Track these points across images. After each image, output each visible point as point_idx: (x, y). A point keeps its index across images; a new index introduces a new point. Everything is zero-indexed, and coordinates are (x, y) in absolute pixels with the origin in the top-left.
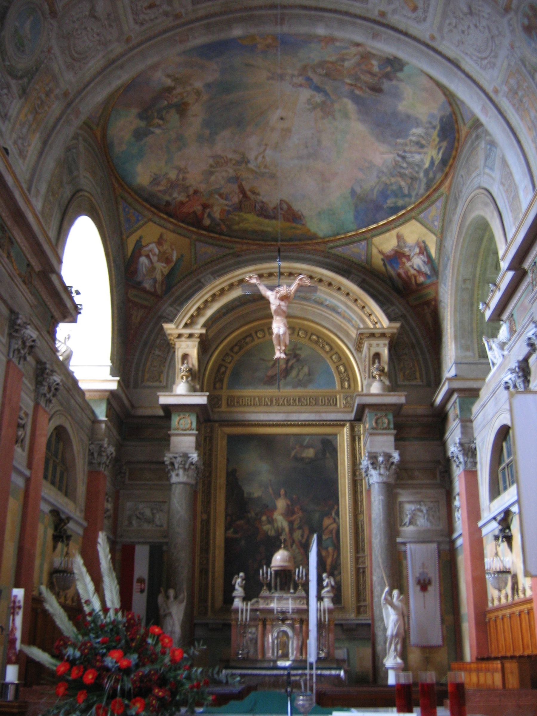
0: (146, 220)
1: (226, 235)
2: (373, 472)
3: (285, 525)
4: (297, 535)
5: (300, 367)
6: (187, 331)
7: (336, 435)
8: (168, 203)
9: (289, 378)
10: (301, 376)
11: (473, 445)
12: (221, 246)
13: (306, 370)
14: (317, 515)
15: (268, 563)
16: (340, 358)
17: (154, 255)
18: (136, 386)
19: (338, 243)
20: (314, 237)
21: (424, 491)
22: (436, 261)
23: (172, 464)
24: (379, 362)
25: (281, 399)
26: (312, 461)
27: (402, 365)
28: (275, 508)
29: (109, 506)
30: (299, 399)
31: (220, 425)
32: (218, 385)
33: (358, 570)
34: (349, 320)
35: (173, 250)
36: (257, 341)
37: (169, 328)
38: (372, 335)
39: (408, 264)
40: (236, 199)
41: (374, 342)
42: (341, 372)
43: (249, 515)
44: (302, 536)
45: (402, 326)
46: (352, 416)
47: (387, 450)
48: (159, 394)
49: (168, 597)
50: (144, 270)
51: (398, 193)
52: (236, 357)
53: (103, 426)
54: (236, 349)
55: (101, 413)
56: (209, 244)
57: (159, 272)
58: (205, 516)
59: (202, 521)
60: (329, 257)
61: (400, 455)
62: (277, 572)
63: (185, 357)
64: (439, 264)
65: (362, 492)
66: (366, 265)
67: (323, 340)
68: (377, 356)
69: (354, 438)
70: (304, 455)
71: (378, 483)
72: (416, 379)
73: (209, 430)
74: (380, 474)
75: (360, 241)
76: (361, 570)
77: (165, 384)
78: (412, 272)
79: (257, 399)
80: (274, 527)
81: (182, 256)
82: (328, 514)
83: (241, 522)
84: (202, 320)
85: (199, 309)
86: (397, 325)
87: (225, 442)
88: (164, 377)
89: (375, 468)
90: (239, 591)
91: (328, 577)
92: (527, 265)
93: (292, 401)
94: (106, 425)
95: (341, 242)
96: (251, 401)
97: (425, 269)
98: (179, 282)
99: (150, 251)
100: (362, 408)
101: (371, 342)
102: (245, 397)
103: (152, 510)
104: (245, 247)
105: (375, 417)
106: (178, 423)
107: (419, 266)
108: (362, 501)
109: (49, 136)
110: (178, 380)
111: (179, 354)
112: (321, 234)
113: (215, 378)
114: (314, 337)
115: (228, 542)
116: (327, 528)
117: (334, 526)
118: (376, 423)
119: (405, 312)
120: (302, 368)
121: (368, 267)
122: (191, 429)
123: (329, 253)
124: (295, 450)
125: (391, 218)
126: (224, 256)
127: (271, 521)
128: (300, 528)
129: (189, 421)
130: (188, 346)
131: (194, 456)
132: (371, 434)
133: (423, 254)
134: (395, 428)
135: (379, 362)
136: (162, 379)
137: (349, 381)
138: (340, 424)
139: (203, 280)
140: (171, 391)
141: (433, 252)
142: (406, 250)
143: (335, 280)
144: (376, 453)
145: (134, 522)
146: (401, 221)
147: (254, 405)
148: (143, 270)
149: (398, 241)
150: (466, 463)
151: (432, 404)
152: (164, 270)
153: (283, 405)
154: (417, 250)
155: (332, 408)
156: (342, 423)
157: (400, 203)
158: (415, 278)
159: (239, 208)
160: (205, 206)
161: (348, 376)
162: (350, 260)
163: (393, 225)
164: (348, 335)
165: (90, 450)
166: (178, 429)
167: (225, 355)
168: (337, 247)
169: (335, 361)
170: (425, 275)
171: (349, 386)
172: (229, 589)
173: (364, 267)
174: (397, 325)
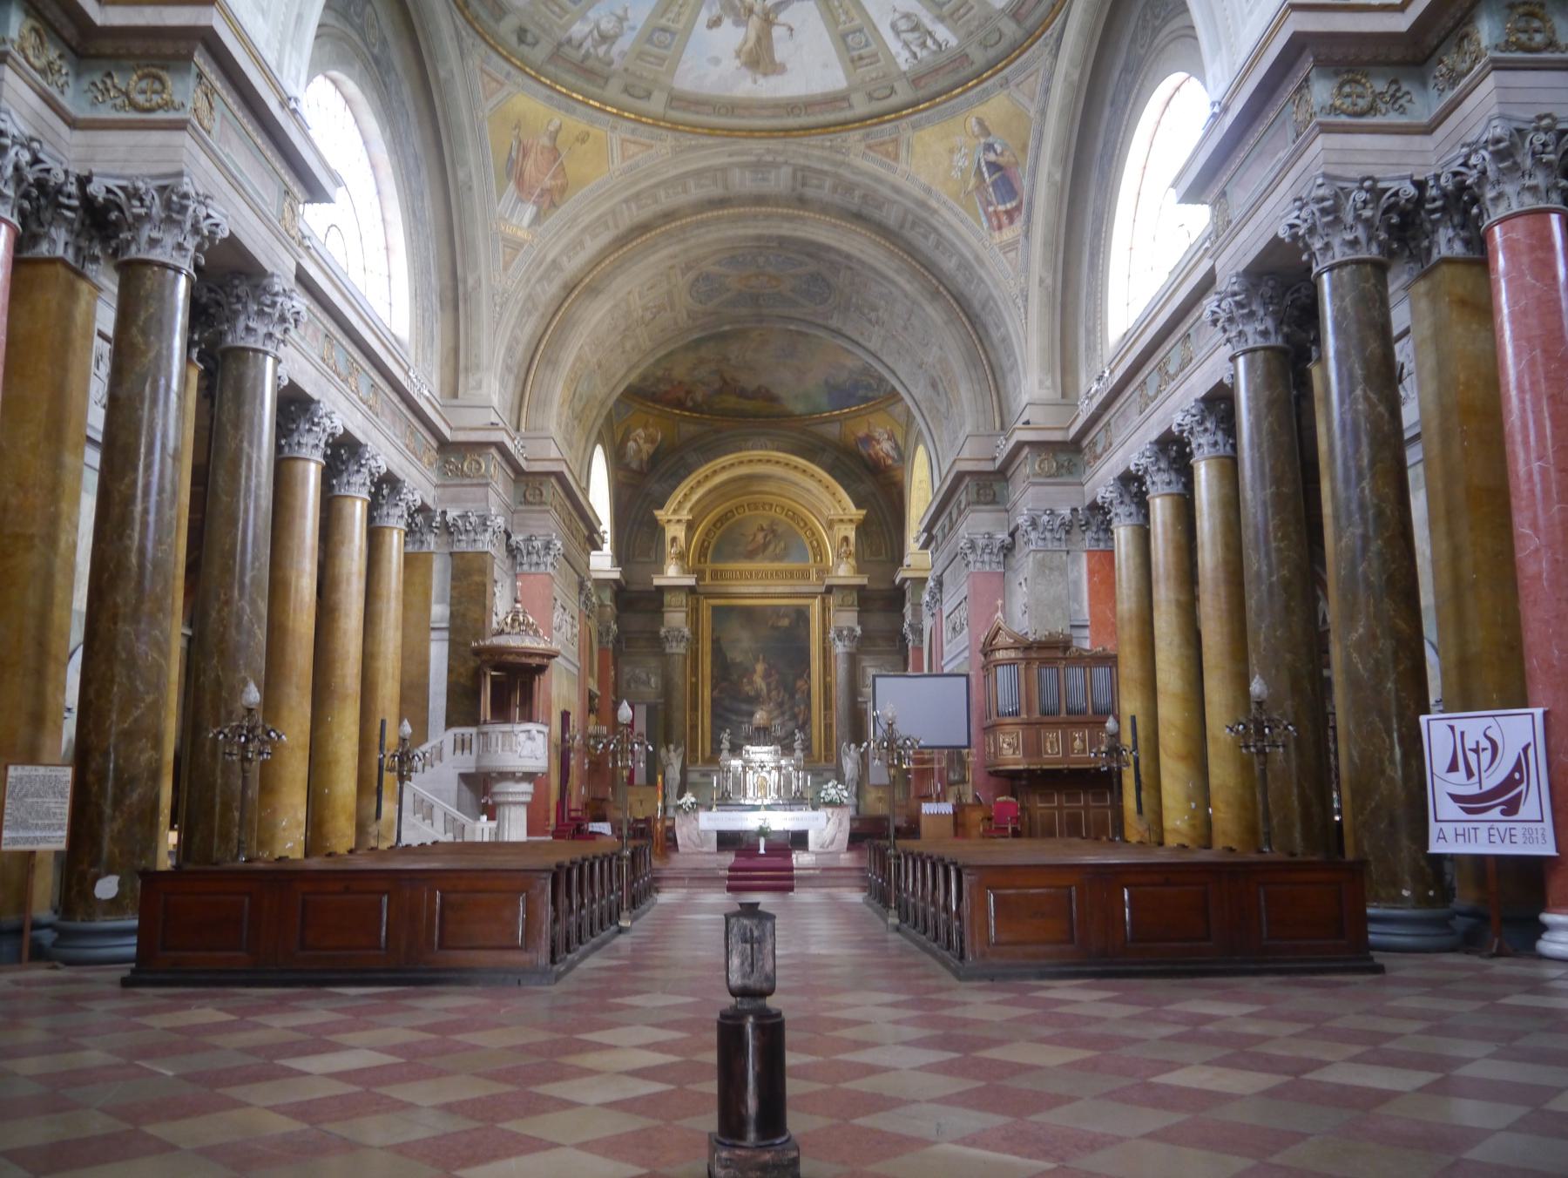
2: (838, 643)
3: (764, 686)
4: (774, 693)
7: (808, 606)
8: (654, 393)
10: (778, 551)
13: (782, 544)
15: (750, 723)
16: (813, 534)
20: (789, 415)
28: (755, 671)
29: (613, 673)
33: (825, 725)
36: (737, 517)
37: (660, 515)
38: (842, 521)
40: (717, 386)
41: (843, 527)
45: (866, 517)
46: (823, 589)
47: (850, 624)
49: (668, 751)
51: (868, 387)
52: (719, 533)
55: (607, 597)
58: (694, 680)
63: (674, 539)
68: (846, 539)
69: (825, 609)
70: (780, 624)
78: (881, 454)
82: (801, 676)
83: (724, 684)
84: (688, 505)
86: (864, 512)
87: (710, 613)
90: (726, 745)
92: (934, 532)
97: (892, 453)
100: (830, 590)
110: (668, 561)
111: (668, 536)
112: (797, 412)
115: (715, 702)
122: (681, 606)
127: (751, 682)
128: (776, 688)
131: (686, 631)
134: (859, 605)
138: (813, 596)
141: (900, 442)
153: (762, 578)
155: (802, 582)
157: (870, 394)
159: (720, 391)
160: (688, 392)
164: (821, 513)
167: (707, 533)
170: (893, 458)
172: (716, 742)
174: (864, 512)
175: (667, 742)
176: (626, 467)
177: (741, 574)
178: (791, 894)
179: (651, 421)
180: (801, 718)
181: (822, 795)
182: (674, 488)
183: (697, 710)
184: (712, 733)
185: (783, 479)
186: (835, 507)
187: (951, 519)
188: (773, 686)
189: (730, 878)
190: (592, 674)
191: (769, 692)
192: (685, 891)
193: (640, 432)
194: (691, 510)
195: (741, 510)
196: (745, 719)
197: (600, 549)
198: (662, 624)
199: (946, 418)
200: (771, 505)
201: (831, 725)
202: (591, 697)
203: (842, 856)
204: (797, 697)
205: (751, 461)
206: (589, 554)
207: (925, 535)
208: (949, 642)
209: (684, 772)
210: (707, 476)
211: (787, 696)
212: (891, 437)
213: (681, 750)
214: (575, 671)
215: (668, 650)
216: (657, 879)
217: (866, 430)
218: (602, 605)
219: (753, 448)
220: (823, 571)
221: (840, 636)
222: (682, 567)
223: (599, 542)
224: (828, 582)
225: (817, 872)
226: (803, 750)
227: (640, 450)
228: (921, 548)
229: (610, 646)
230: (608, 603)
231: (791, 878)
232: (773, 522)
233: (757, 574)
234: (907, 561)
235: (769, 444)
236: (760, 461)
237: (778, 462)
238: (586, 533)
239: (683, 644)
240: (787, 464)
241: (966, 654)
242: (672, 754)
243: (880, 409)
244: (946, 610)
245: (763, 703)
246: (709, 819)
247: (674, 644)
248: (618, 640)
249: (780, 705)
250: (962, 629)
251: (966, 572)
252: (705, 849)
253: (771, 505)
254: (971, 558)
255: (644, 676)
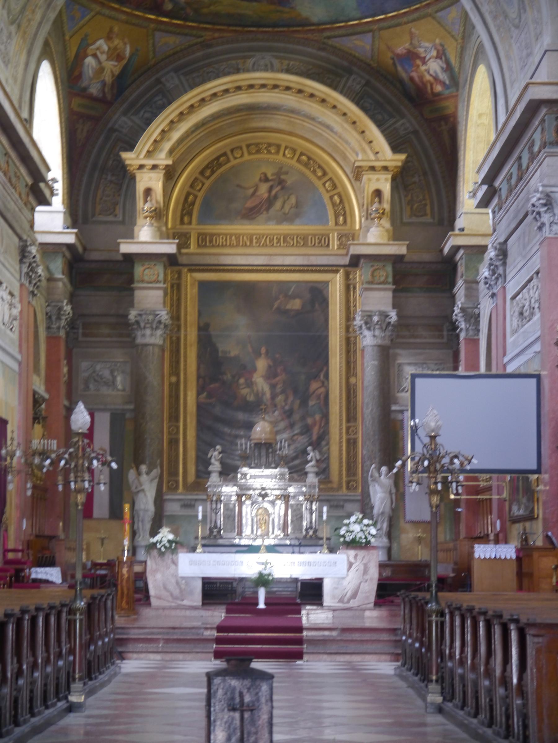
0: (92, 14)
1: (192, 21)
2: (366, 333)
3: (267, 389)
4: (280, 399)
5: (286, 197)
6: (150, 162)
7: (326, 283)
9: (272, 211)
10: (287, 208)
11: (476, 311)
12: (186, 35)
13: (293, 200)
14: (303, 377)
16: (335, 187)
17: (103, 53)
18: (86, 221)
19: (337, 33)
20: (305, 23)
21: (427, 351)
22: (456, 70)
23: (137, 322)
24: (380, 202)
25: (263, 237)
26: (298, 313)
27: (410, 196)
28: (255, 370)
29: (65, 370)
30: (284, 238)
31: (190, 271)
32: (186, 219)
33: (348, 441)
34: (347, 142)
35: (125, 44)
36: (233, 162)
37: (129, 157)
38: (373, 168)
39: (423, 68)
41: (374, 176)
42: (336, 203)
43: (225, 377)
44: (286, 400)
45: (406, 163)
46: (346, 261)
47: (383, 308)
48: (119, 241)
49: (139, 474)
50: (90, 72)
52: (208, 183)
53: (60, 284)
54: (208, 173)
56: (171, 32)
57: (109, 71)
58: (174, 379)
59: (170, 384)
60: (323, 49)
61: (398, 315)
62: (256, 444)
63: (148, 192)
64: (459, 73)
65: (355, 351)
66: (371, 62)
67: (314, 161)
68: (378, 193)
69: (349, 287)
70: (289, 307)
71: (371, 346)
72: (425, 215)
73: (176, 276)
74: (374, 336)
75: (364, 32)
76: (352, 441)
77: (121, 219)
78: (428, 77)
79: (233, 238)
80: (253, 391)
81: (137, 50)
82: (316, 377)
84: (167, 146)
85: (163, 131)
86: (403, 157)
87: (195, 290)
88: (119, 210)
89: (369, 329)
90: (215, 466)
91: (314, 450)
92: (497, 184)
93: (275, 241)
94: (64, 284)
95: (340, 32)
96: (226, 240)
97: (443, 76)
98: (132, 83)
99: (98, 49)
101: (371, 176)
102: (219, 235)
103: (112, 372)
104: (216, 35)
105: (372, 269)
106: (143, 274)
107: (435, 72)
108: (355, 362)
109: (32, 44)
110: (140, 221)
111: (140, 187)
112: (315, 20)
113: (183, 210)
114: (304, 158)
115: (200, 407)
116: (314, 392)
117: (322, 390)
118: (373, 275)
119: (417, 127)
120: (288, 198)
121: (375, 65)
122: (158, 282)
123: (324, 43)
124: (279, 301)
125: (403, 11)
126: (190, 46)
127: (250, 384)
129: (156, 273)
130: (150, 179)
131: (164, 315)
132: (366, 289)
133: (441, 59)
134: (395, 282)
135: (380, 202)
136: (117, 211)
137: (344, 215)
138: (332, 269)
139: (163, 80)
140: (132, 237)
142: (421, 50)
143: (329, 96)
144: (371, 311)
145: (91, 386)
146: (416, 15)
147: (230, 245)
148: (88, 71)
149: (411, 40)
150: (467, 330)
151: (441, 251)
152: (114, 69)
153: (265, 245)
154: (434, 53)
156: (334, 268)
158: (432, 85)
161: (344, 208)
162: (351, 54)
163: (405, 19)
164: (345, 158)
165: (47, 314)
166: (143, 281)
168: (335, 37)
169: (329, 189)
170: (443, 84)
171: (345, 221)
173: (369, 65)
174: (403, 157)
175: (138, 461)
176: (83, 93)
177: (237, 238)
178: (299, 662)
179: (116, 29)
180: (315, 431)
181: (342, 532)
182: (148, 122)
183: (177, 419)
184: (198, 450)
185: (293, 111)
186: (364, 151)
187: (520, 166)
188: (279, 389)
189: (218, 641)
190: (36, 370)
191: (273, 397)
192: (158, 657)
193: (102, 44)
194: (171, 152)
195: (237, 154)
196: (242, 433)
197: (48, 203)
198: (131, 304)
199: (517, 27)
200: (278, 147)
201: (355, 442)
202: (37, 401)
203: (368, 613)
204: (311, 403)
205: (251, 86)
206: (33, 210)
207: (485, 187)
208: (514, 332)
209: (159, 501)
210: (192, 106)
211: (298, 402)
212: (441, 55)
213: (156, 472)
214: (15, 366)
215: (139, 340)
216: (122, 642)
217: (407, 45)
218: (51, 279)
219: (255, 68)
220: (347, 236)
221: (368, 323)
222: (159, 229)
223: (47, 192)
224: (355, 250)
225: (334, 633)
226: (317, 474)
227: (101, 70)
228: (479, 206)
229: (62, 333)
230: (59, 276)
231: (300, 641)
232: (281, 172)
233: (258, 239)
234: (460, 223)
235: (276, 62)
236: (263, 86)
237: (288, 88)
238: (30, 181)
239: (159, 332)
240: (300, 91)
241: (537, 347)
242: (144, 478)
243: (430, 15)
244: (512, 288)
245: (265, 411)
246: (192, 563)
247: (148, 332)
248: (72, 325)
249: (289, 414)
250: (532, 314)
251: (538, 238)
252: (186, 602)
253: (278, 147)
254: (546, 218)
255: (106, 373)
